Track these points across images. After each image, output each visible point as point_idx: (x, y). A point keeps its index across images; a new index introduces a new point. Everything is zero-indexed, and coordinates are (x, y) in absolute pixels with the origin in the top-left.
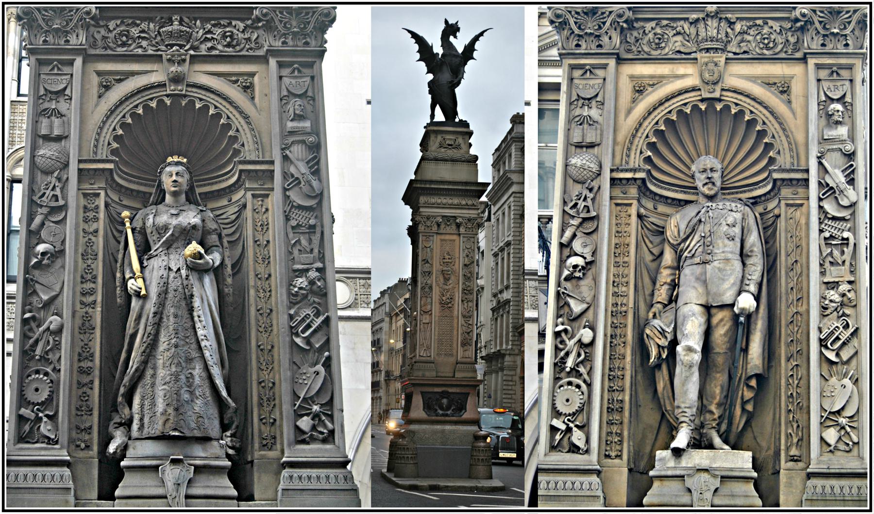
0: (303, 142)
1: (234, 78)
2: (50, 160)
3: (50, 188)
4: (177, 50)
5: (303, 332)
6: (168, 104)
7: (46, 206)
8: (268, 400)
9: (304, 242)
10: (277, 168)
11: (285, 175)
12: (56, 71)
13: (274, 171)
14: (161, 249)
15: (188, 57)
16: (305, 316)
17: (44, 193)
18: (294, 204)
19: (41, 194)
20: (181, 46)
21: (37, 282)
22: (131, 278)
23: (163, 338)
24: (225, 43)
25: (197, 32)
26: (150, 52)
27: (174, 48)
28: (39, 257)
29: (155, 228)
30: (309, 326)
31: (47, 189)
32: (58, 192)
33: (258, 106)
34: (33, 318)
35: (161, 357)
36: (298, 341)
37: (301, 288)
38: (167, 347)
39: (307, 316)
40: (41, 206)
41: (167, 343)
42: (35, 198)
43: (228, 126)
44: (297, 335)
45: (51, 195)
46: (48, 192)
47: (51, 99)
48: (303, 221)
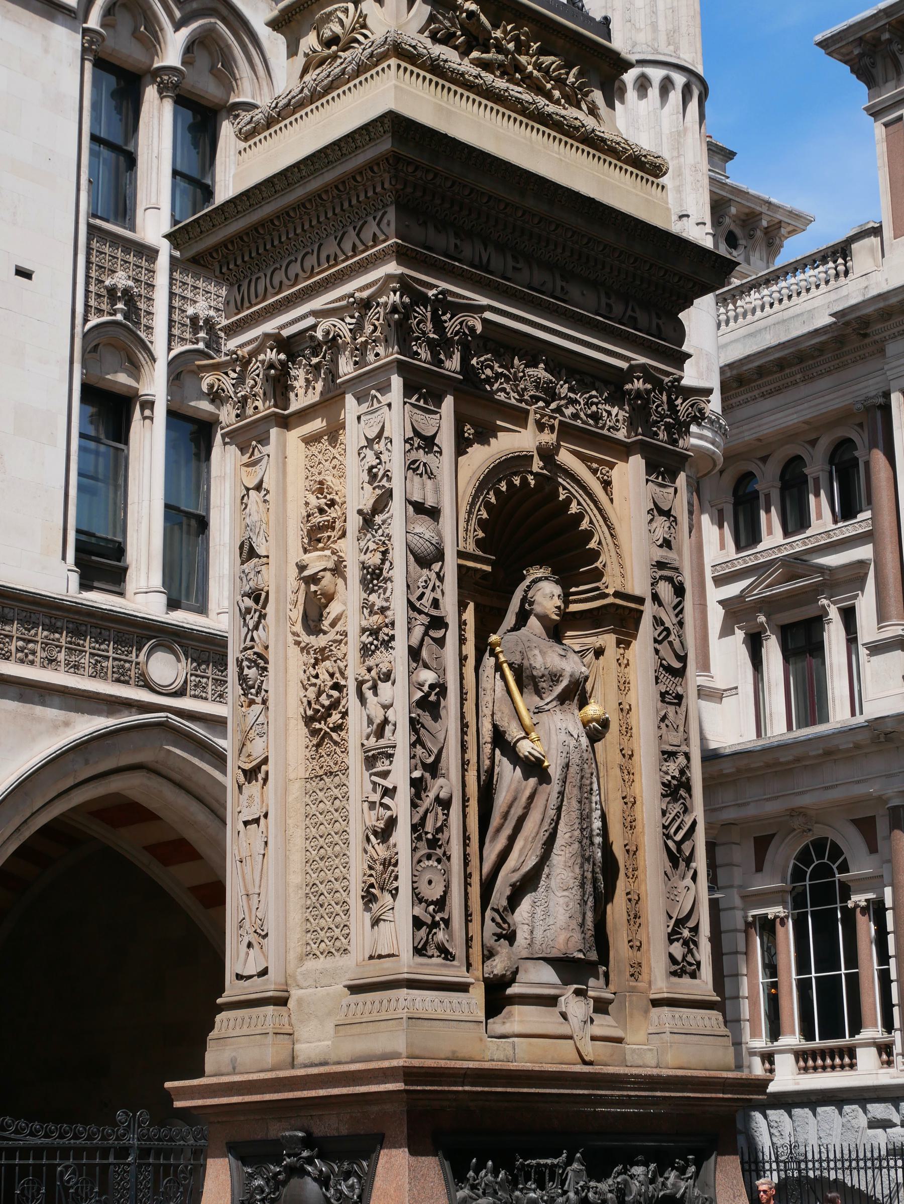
0: (670, 580)
1: (595, 465)
2: (429, 545)
3: (430, 587)
4: (543, 408)
5: (676, 833)
6: (532, 486)
7: (427, 614)
8: (635, 918)
9: (671, 715)
10: (649, 609)
11: (658, 621)
12: (422, 403)
13: (642, 612)
14: (554, 703)
15: (556, 423)
16: (676, 815)
17: (423, 594)
18: (664, 662)
19: (418, 593)
20: (548, 404)
21: (423, 726)
22: (524, 738)
23: (562, 828)
24: (589, 412)
25: (562, 386)
26: (513, 401)
27: (541, 404)
28: (426, 688)
29: (546, 673)
30: (679, 828)
31: (427, 588)
32: (438, 595)
33: (618, 511)
34: (421, 779)
35: (563, 853)
36: (670, 843)
37: (673, 777)
38: (570, 840)
39: (677, 815)
40: (420, 612)
41: (568, 835)
42: (413, 599)
43: (589, 535)
44: (668, 836)
45: (431, 598)
46: (428, 591)
47: (419, 447)
48: (671, 688)
